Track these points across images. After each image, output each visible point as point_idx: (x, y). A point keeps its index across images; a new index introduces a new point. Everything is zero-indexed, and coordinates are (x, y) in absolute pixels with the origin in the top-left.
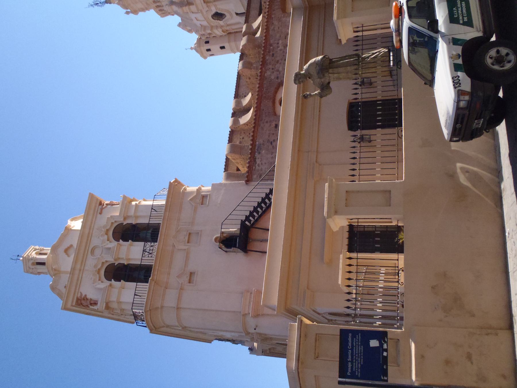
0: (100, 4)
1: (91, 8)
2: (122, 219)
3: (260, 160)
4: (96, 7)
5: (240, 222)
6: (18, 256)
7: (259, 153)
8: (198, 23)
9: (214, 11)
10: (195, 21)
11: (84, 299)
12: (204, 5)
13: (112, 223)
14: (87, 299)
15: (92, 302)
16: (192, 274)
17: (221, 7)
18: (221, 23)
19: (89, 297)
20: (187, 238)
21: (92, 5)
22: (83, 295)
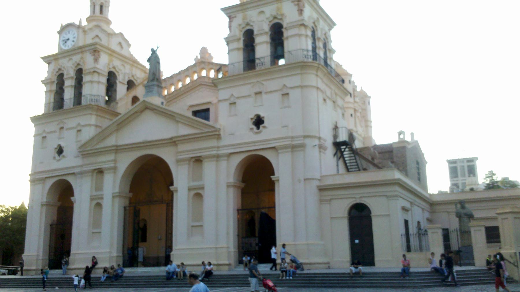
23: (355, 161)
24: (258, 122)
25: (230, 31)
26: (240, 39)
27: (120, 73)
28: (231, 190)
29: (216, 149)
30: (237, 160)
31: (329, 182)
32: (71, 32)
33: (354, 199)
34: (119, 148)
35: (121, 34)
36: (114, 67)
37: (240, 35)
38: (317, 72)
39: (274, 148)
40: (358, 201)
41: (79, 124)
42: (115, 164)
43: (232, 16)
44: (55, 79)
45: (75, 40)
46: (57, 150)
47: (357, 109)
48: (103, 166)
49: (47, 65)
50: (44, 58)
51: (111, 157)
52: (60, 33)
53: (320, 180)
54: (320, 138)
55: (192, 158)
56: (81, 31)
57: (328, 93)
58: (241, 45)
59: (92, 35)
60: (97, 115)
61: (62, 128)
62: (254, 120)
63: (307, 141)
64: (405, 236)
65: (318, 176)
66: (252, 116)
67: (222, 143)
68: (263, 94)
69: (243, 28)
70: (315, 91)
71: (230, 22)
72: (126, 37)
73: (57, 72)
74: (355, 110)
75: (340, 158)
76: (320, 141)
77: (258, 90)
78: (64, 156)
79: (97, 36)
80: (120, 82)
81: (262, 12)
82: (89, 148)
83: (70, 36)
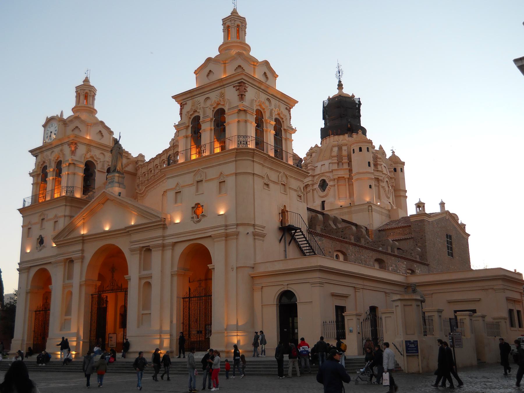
1: (336, 65)
2: (285, 128)
7: (319, 240)
8: (319, 164)
9: (330, 183)
10: (322, 163)
11: (245, 89)
12: (336, 177)
13: (282, 119)
14: (245, 92)
15: (243, 96)
16: (268, 185)
17: (331, 191)
18: (316, 186)
19: (247, 94)
20: (283, 183)
23: (308, 245)
25: (181, 119)
26: (189, 126)
27: (98, 162)
28: (175, 278)
29: (161, 239)
30: (180, 249)
31: (262, 269)
32: (53, 125)
33: (282, 287)
34: (85, 238)
35: (102, 123)
36: (92, 157)
37: (188, 122)
38: (253, 157)
39: (210, 236)
40: (286, 289)
41: (56, 216)
42: (82, 253)
44: (40, 171)
45: (56, 132)
46: (39, 240)
47: (380, 178)
48: (73, 256)
49: (35, 158)
50: (31, 151)
51: (79, 247)
52: (44, 126)
53: (253, 268)
54: (254, 225)
55: (143, 247)
56: (61, 123)
57: (273, 176)
58: (189, 133)
59: (72, 126)
60: (71, 206)
61: (43, 219)
63: (241, 229)
64: (335, 323)
65: (251, 263)
67: (169, 232)
68: (204, 181)
69: (191, 115)
70: (250, 177)
71: (181, 110)
72: (107, 124)
73: (42, 165)
74: (377, 180)
75: (290, 243)
77: (199, 179)
78: (44, 247)
79: (77, 127)
80: (98, 171)
81: (208, 98)
82: (62, 239)
83: (52, 129)
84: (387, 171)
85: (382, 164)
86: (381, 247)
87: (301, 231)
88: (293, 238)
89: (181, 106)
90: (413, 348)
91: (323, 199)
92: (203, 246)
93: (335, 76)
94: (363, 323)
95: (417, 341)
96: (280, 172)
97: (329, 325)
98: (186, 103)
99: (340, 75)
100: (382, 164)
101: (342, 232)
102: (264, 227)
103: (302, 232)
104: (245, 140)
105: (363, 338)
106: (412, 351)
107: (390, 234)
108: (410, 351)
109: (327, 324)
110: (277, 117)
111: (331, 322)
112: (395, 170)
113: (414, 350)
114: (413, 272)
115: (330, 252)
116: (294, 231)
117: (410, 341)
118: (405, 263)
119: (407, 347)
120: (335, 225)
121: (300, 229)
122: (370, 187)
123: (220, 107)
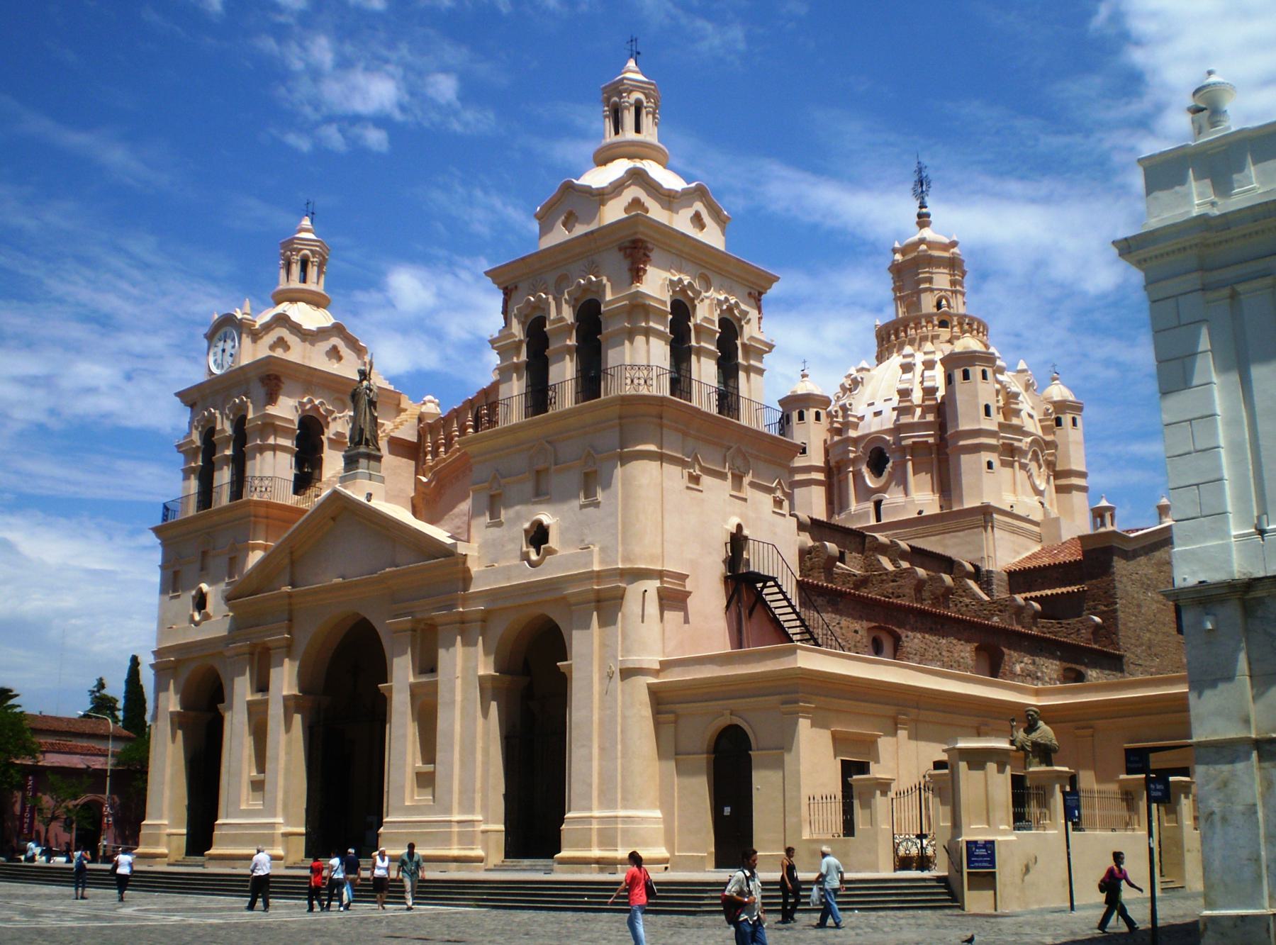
0: (920, 190)
1: (915, 167)
3: (822, 603)
4: (916, 178)
5: (775, 576)
6: (638, 53)
7: (828, 602)
21: (920, 170)
22: (650, 254)
24: (539, 536)
43: (509, 287)
47: (1016, 444)
54: (660, 575)
62: (532, 533)
66: (527, 525)
76: (662, 582)
84: (1035, 425)
85: (1020, 410)
86: (998, 615)
87: (777, 585)
88: (759, 601)
89: (505, 294)
90: (983, 856)
91: (876, 497)
92: (551, 621)
93: (912, 193)
94: (894, 801)
95: (992, 842)
96: (729, 448)
97: (820, 805)
98: (516, 287)
99: (924, 189)
100: (1020, 410)
101: (893, 581)
102: (683, 577)
103: (779, 587)
104: (641, 375)
105: (894, 835)
106: (980, 864)
107: (1036, 581)
108: (977, 864)
109: (816, 801)
110: (727, 316)
111: (824, 798)
112: (1058, 422)
113: (986, 861)
114: (1080, 677)
115: (856, 632)
116: (760, 585)
117: (975, 842)
118: (1059, 653)
119: (970, 854)
120: (893, 561)
121: (773, 579)
122: (990, 465)
123: (589, 297)
